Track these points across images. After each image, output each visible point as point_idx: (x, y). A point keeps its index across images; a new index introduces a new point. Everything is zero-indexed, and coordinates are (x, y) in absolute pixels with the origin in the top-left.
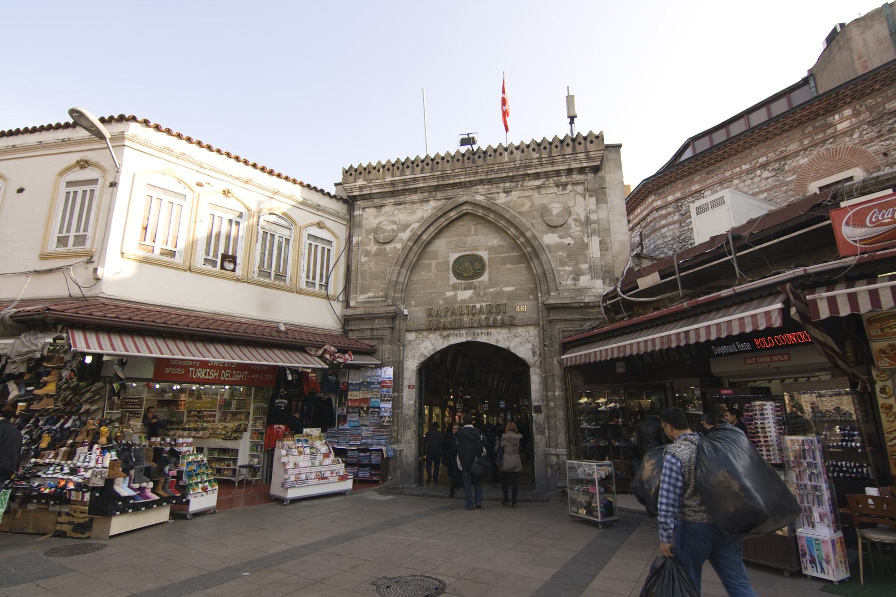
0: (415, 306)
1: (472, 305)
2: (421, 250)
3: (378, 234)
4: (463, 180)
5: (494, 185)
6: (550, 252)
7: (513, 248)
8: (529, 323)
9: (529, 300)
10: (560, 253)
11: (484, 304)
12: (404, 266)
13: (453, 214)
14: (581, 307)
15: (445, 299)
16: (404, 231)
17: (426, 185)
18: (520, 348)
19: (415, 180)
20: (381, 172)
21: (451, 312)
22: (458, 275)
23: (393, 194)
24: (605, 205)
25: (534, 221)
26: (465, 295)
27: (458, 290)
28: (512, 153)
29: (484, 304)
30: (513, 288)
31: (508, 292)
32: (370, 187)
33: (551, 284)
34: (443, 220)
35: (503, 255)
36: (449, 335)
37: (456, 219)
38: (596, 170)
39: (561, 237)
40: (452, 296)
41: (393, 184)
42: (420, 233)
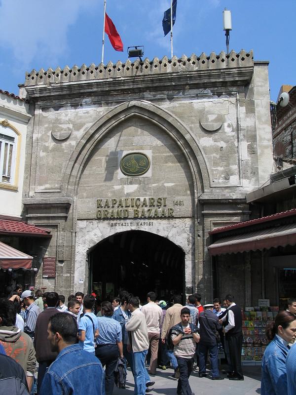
0: (87, 198)
1: (137, 198)
2: (93, 147)
3: (55, 132)
4: (131, 87)
5: (159, 92)
6: (206, 154)
7: (175, 148)
8: (186, 216)
9: (186, 195)
10: (214, 155)
11: (147, 198)
12: (78, 161)
13: (122, 117)
15: (114, 192)
16: (78, 129)
17: (99, 89)
18: (177, 237)
19: (90, 85)
20: (59, 76)
21: (118, 203)
27: (125, 184)
29: (147, 198)
30: (173, 184)
31: (168, 188)
33: (206, 183)
36: (115, 225)
39: (215, 141)
40: (120, 189)
41: (70, 87)
42: (93, 132)
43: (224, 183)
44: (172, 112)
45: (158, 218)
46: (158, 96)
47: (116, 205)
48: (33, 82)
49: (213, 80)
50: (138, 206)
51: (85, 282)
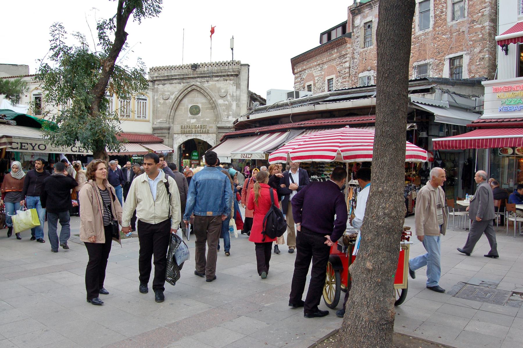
4: (192, 76)
9: (214, 124)
10: (224, 107)
11: (199, 125)
13: (189, 89)
14: (227, 128)
15: (187, 122)
16: (172, 95)
17: (179, 77)
19: (175, 75)
22: (191, 113)
23: (168, 80)
24: (239, 89)
25: (216, 94)
26: (193, 121)
28: (208, 67)
29: (199, 125)
32: (160, 77)
34: (186, 91)
35: (206, 106)
37: (191, 91)
38: (237, 75)
39: (224, 101)
41: (168, 76)
43: (227, 119)
44: (208, 88)
45: (203, 133)
46: (203, 81)
47: (188, 128)
48: (152, 73)
49: (223, 74)
50: (196, 128)
51: (177, 159)
